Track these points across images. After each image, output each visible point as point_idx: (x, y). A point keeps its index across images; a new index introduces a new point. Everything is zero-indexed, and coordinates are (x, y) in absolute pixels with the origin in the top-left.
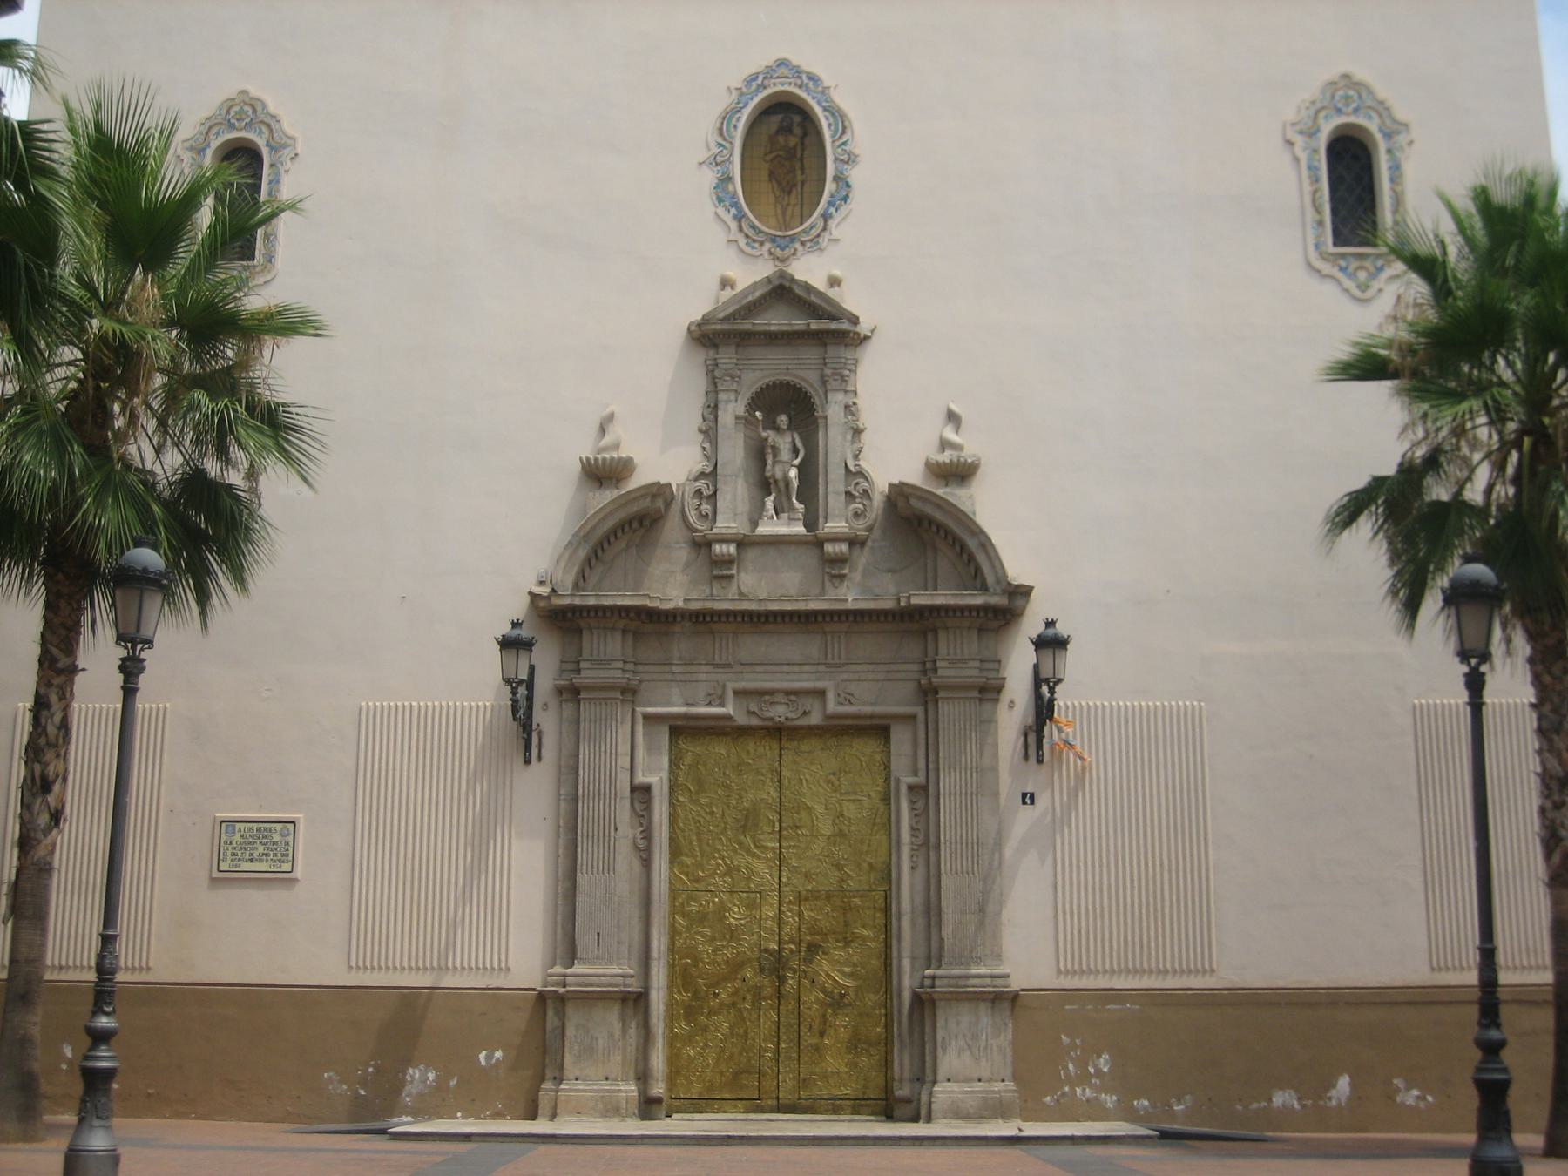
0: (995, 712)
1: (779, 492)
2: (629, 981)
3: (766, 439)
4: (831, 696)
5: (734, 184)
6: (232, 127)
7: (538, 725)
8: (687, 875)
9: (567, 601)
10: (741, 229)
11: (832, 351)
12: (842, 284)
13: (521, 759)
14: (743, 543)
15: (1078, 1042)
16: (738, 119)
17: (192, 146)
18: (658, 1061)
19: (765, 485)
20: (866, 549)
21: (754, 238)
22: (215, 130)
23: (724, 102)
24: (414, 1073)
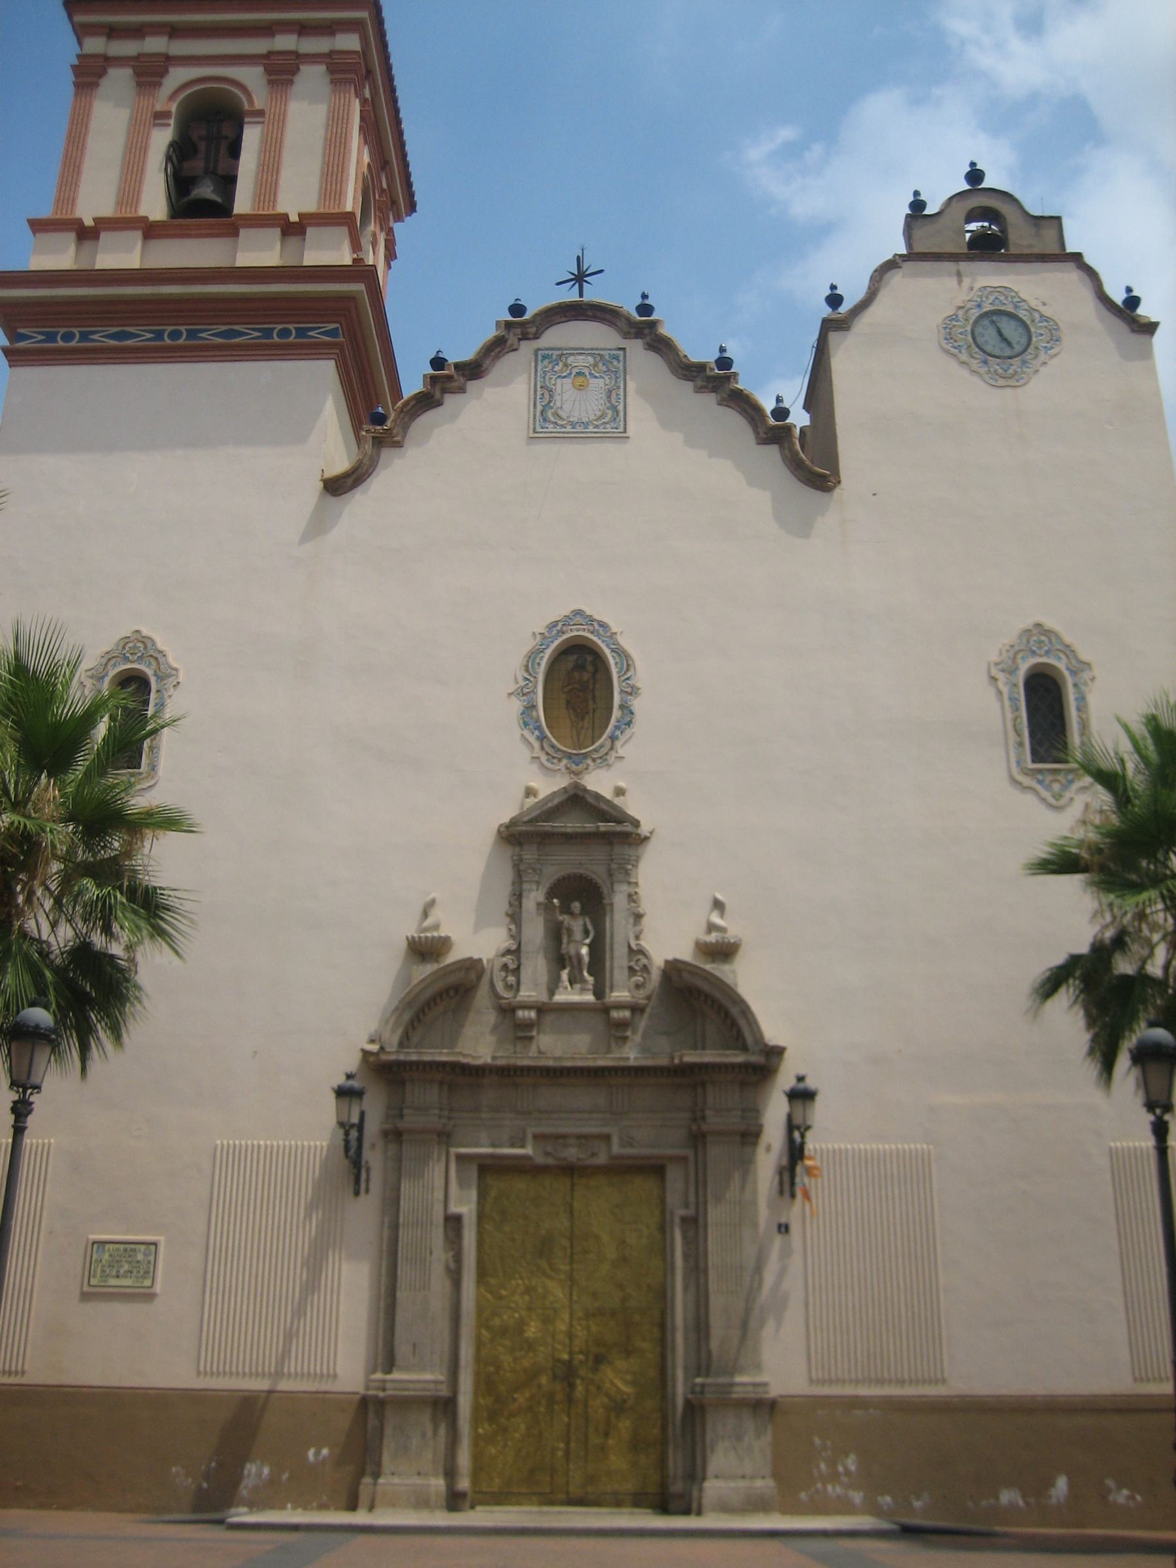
0: (754, 1153)
1: (572, 967)
2: (440, 1387)
3: (562, 922)
4: (615, 1140)
5: (537, 711)
6: (126, 660)
7: (367, 1162)
8: (491, 1293)
9: (393, 1057)
10: (542, 748)
11: (617, 849)
12: (627, 794)
13: (351, 1191)
14: (542, 1009)
15: (829, 1443)
16: (541, 658)
17: (93, 674)
18: (464, 1459)
19: (560, 960)
20: (646, 1015)
21: (554, 755)
22: (112, 662)
23: (530, 644)
24: (251, 1468)
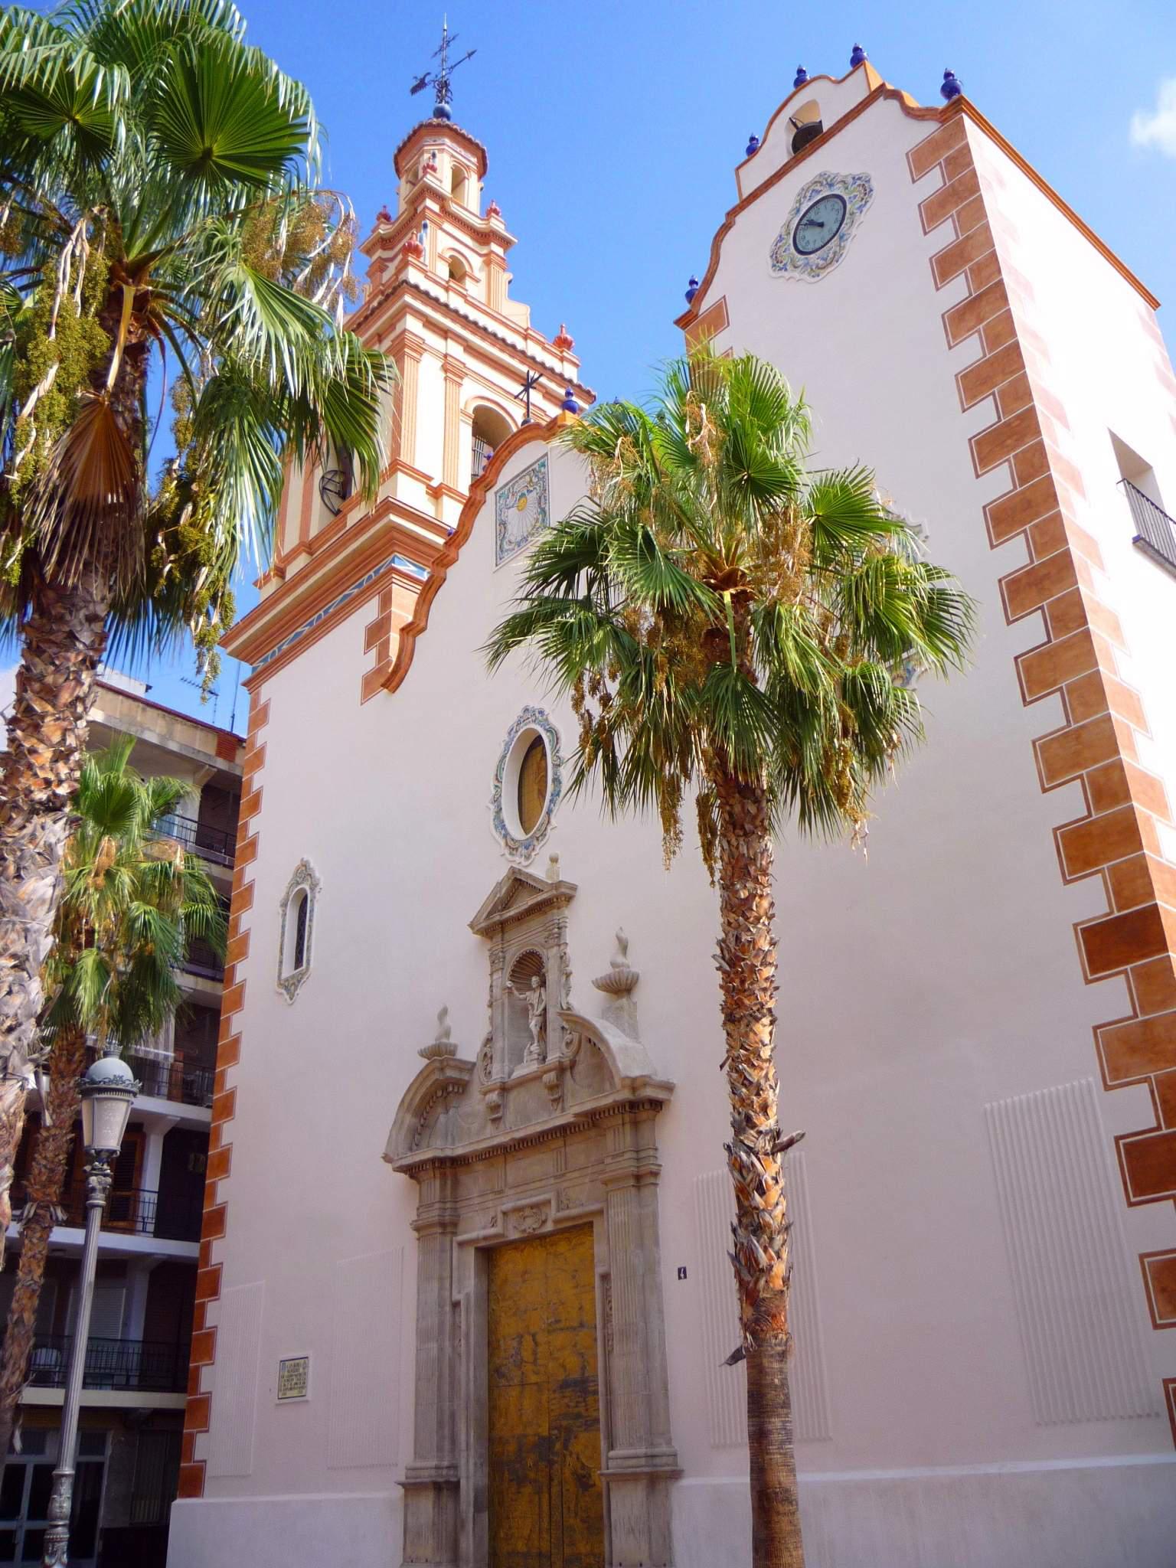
10: (507, 844)
